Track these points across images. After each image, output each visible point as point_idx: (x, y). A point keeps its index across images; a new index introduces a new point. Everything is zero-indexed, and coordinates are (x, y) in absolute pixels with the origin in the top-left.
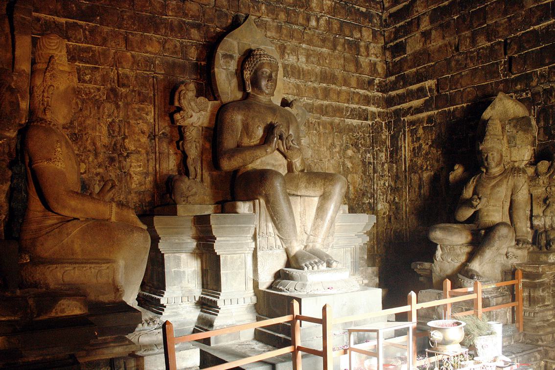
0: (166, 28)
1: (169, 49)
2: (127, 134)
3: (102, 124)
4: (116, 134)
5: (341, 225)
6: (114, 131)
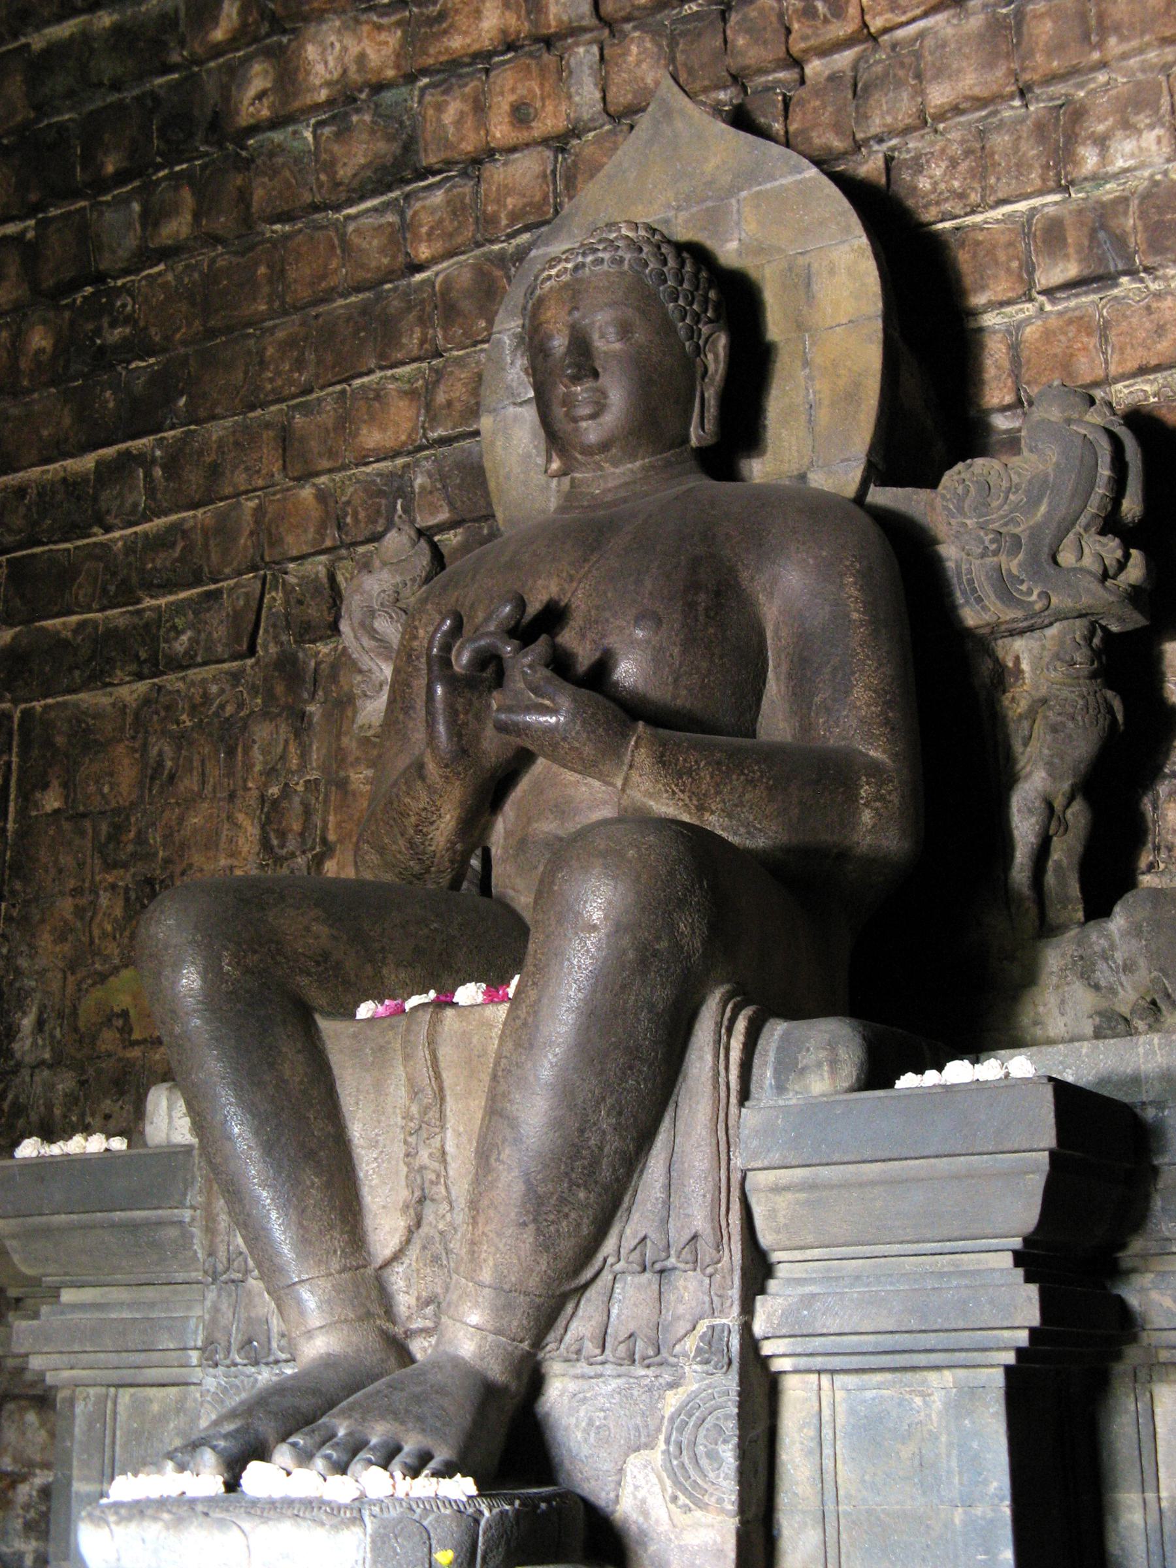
0: (423, 321)
1: (449, 404)
2: (332, 837)
3: (241, 817)
4: (292, 844)
5: (810, 1186)
6: (282, 835)
